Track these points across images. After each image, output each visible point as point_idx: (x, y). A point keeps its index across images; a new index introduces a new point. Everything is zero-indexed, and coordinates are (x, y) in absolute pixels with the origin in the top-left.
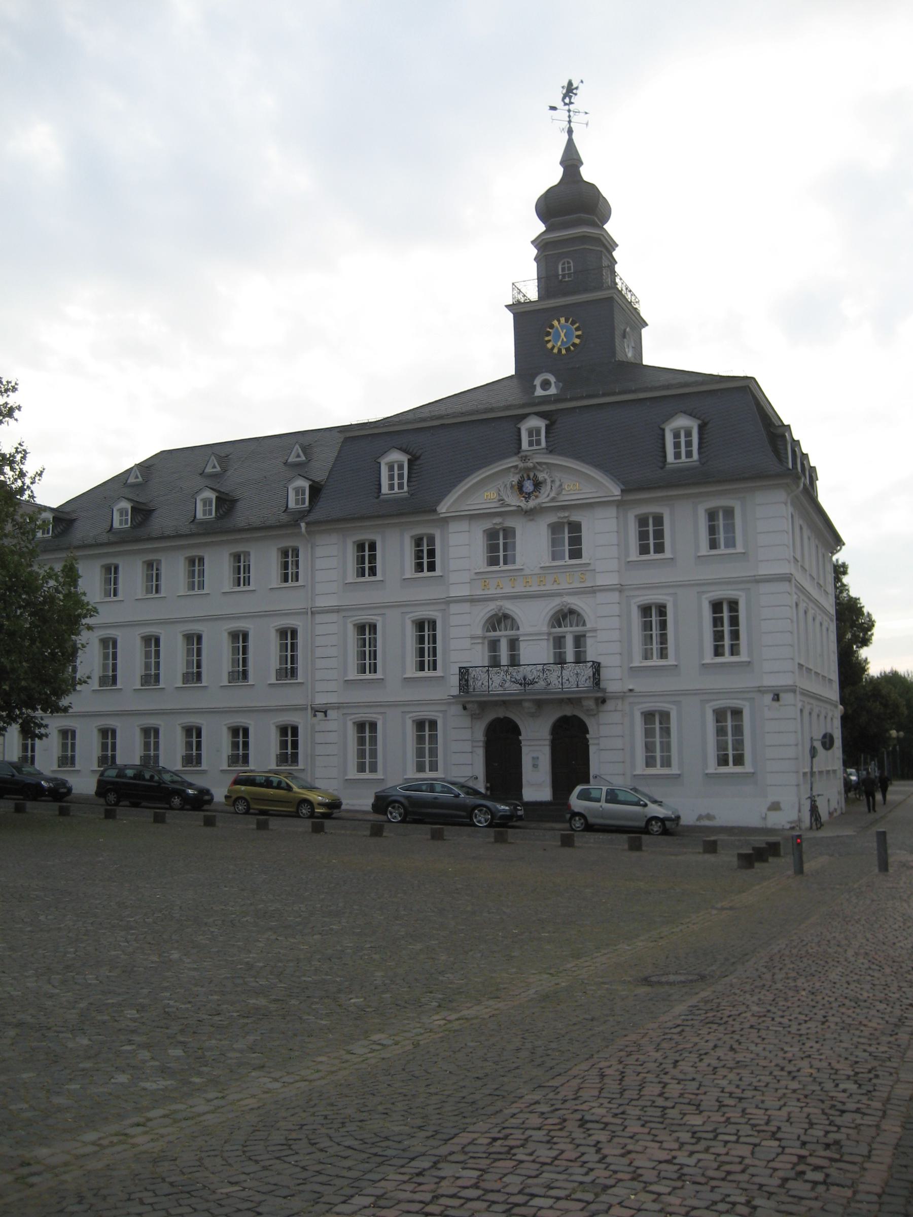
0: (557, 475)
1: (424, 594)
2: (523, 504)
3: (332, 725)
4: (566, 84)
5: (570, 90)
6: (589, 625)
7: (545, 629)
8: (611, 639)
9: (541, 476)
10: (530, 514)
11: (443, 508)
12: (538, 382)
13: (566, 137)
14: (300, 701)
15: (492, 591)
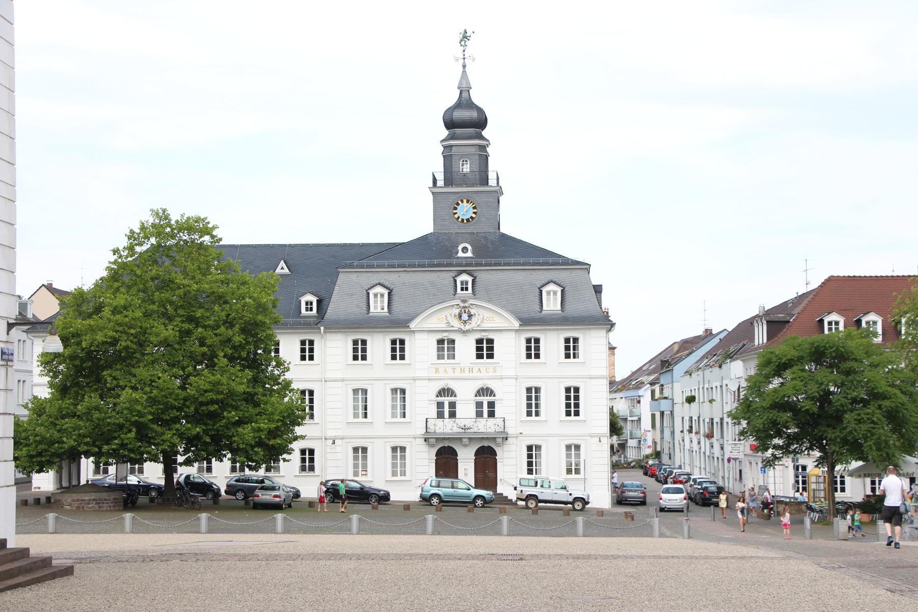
0: (482, 312)
1: (398, 373)
2: (463, 327)
3: (339, 449)
4: (463, 32)
5: (465, 37)
6: (497, 397)
7: (473, 397)
8: (510, 405)
9: (473, 311)
10: (465, 332)
11: (413, 325)
12: (460, 248)
13: (462, 69)
14: (318, 434)
15: (441, 375)
